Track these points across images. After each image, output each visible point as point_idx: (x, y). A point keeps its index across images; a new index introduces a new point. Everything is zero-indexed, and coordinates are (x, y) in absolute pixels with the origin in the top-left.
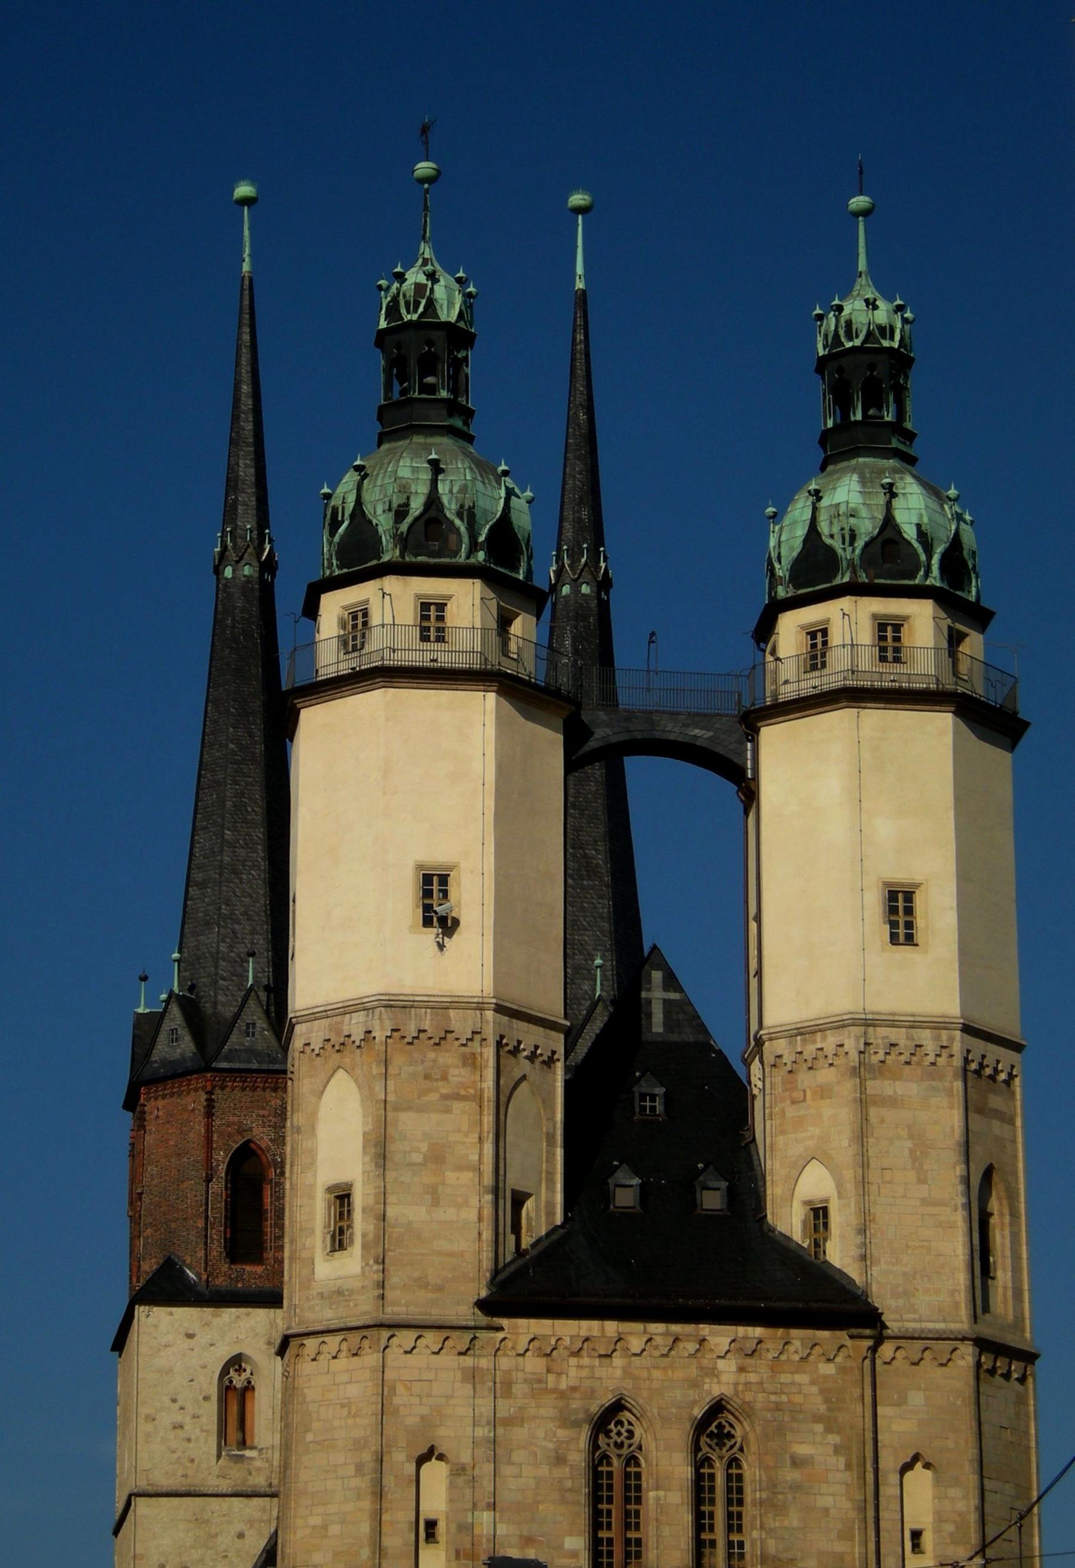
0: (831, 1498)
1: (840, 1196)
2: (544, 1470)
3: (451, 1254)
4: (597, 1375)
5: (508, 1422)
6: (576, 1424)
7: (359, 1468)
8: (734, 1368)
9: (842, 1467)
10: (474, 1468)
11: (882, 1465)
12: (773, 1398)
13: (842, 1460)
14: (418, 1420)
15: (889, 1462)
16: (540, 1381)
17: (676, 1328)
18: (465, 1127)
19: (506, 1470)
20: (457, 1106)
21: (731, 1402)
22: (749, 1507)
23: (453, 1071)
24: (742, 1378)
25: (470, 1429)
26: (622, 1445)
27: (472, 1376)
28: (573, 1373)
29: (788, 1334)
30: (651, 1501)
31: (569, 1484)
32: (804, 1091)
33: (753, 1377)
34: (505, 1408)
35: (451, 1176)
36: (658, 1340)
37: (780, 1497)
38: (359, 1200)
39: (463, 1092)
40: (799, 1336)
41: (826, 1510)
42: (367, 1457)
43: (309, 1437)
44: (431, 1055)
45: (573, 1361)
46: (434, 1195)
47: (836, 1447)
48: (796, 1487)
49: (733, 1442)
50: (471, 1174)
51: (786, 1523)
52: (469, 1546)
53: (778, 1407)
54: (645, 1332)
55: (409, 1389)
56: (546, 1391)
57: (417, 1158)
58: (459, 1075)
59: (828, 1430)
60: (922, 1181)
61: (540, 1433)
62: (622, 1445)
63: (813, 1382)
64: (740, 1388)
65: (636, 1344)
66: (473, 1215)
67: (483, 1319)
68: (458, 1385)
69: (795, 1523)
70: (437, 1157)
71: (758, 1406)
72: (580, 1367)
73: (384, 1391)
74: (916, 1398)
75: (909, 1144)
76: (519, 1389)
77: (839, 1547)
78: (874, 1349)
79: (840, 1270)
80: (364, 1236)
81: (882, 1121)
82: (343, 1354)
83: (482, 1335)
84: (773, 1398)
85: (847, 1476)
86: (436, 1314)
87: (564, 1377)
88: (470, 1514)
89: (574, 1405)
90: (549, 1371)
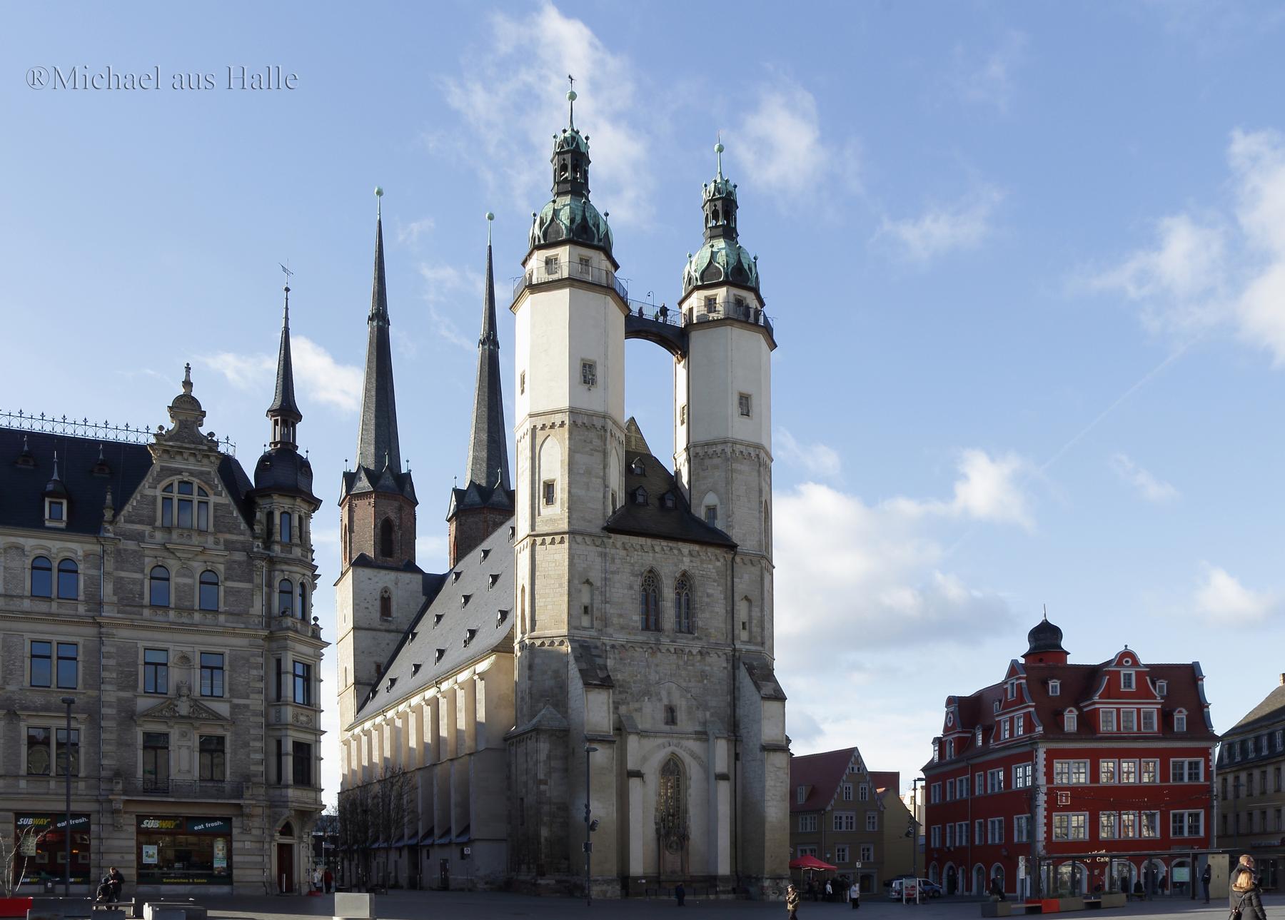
1: (721, 504)
3: (593, 509)
5: (613, 573)
6: (637, 576)
7: (561, 585)
8: (688, 561)
11: (735, 599)
12: (701, 572)
15: (736, 598)
17: (670, 544)
19: (613, 590)
27: (604, 556)
28: (636, 557)
31: (634, 597)
33: (695, 565)
34: (613, 568)
35: (594, 479)
36: (665, 548)
40: (711, 550)
41: (718, 613)
45: (636, 552)
48: (708, 604)
55: (579, 557)
56: (627, 562)
57: (582, 472)
59: (718, 585)
60: (749, 501)
63: (714, 568)
65: (657, 549)
69: (708, 616)
72: (637, 555)
74: (746, 577)
78: (733, 559)
79: (720, 531)
80: (561, 499)
81: (737, 479)
83: (605, 540)
85: (724, 602)
89: (636, 569)
90: (627, 556)
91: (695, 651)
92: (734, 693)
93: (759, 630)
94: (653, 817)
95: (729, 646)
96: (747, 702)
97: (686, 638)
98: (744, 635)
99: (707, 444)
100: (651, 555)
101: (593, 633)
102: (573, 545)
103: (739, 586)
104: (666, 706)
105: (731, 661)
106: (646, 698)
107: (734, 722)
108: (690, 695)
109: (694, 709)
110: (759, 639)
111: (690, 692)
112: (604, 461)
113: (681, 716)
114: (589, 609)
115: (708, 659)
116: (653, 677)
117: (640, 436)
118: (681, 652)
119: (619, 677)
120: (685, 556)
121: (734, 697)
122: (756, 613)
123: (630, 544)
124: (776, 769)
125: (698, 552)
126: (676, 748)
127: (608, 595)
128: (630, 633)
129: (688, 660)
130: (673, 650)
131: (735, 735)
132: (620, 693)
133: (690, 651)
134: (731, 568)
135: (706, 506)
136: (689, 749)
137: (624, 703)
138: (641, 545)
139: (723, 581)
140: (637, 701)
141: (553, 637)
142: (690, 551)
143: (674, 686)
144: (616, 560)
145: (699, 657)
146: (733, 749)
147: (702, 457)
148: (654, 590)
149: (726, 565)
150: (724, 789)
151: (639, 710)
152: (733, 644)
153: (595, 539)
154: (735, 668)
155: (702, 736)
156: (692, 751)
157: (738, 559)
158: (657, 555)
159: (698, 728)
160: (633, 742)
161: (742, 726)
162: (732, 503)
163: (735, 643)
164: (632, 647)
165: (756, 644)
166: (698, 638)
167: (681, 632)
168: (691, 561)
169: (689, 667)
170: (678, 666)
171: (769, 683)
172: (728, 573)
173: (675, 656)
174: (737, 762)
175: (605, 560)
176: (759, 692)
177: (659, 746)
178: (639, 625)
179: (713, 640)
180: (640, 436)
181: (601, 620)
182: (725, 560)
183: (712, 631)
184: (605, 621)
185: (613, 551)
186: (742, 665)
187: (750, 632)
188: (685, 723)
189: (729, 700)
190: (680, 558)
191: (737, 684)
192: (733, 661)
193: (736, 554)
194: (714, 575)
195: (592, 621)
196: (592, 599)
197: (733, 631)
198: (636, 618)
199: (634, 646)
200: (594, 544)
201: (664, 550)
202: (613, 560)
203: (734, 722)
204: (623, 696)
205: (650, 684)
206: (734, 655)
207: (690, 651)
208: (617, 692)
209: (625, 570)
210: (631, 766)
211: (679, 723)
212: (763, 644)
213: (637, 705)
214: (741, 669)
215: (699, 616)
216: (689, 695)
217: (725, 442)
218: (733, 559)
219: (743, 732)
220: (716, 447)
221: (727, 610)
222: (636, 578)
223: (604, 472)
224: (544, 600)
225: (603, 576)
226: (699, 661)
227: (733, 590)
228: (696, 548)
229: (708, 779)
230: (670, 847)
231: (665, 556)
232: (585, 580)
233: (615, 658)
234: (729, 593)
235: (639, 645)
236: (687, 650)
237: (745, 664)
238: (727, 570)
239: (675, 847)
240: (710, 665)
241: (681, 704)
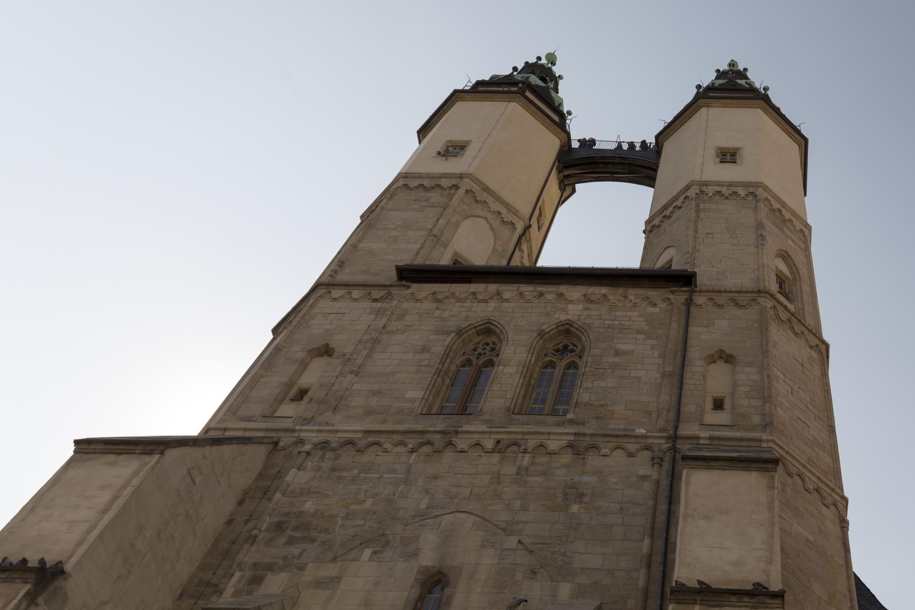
12: (606, 322)
21: (574, 325)
24: (586, 313)
41: (639, 378)
65: (507, 295)
83: (395, 291)
84: (606, 322)
103: (702, 337)
108: (515, 539)
109: (519, 576)
115: (593, 461)
120: (572, 302)
129: (532, 463)
130: (489, 444)
158: (506, 304)
170: (498, 478)
173: (496, 458)
231: (526, 305)
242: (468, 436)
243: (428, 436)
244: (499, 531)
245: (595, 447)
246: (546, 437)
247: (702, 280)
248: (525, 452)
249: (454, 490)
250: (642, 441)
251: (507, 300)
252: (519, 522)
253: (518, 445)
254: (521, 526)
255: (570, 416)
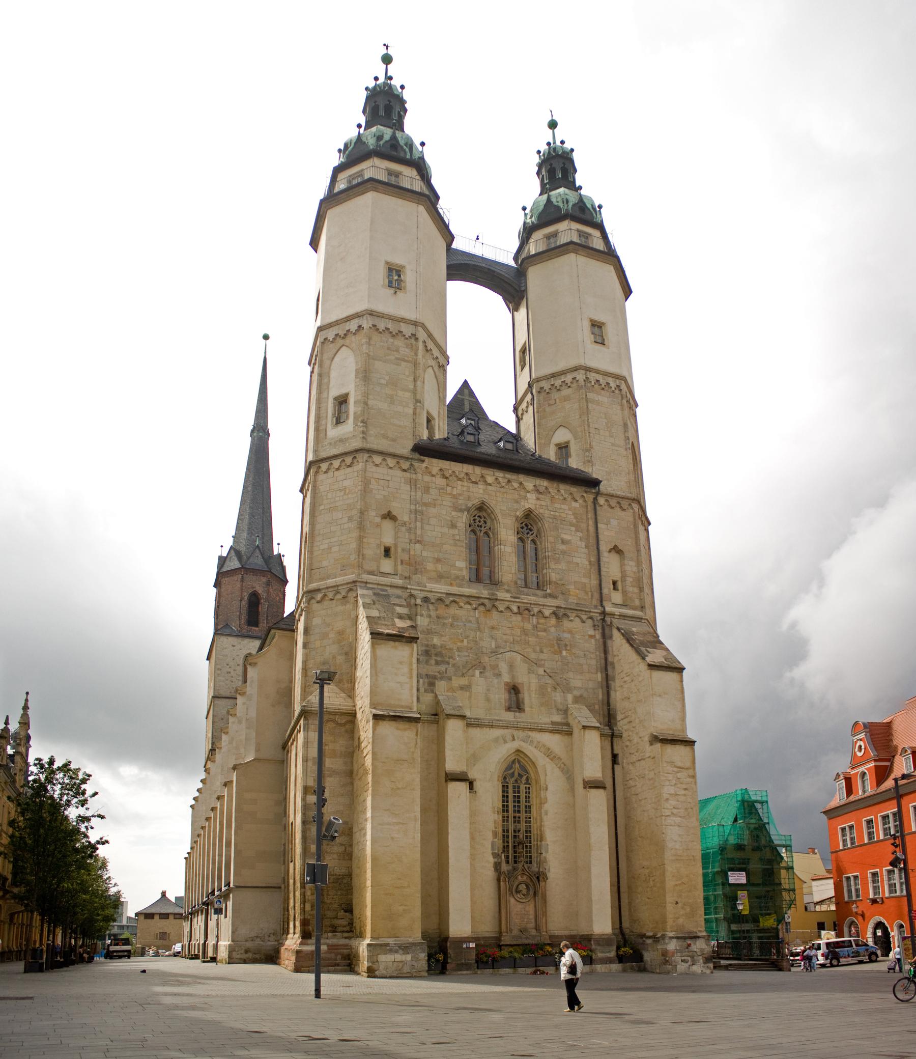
0: (579, 559)
1: (576, 438)
2: (445, 530)
3: (400, 426)
4: (471, 490)
6: (461, 511)
7: (350, 519)
8: (535, 498)
9: (584, 547)
10: (410, 524)
12: (552, 513)
13: (584, 544)
14: (382, 497)
15: (604, 548)
16: (443, 489)
18: (407, 373)
19: (427, 527)
20: (404, 364)
22: (541, 561)
23: (401, 349)
24: (538, 502)
25: (408, 506)
26: (481, 526)
28: (460, 487)
29: (559, 487)
30: (496, 551)
31: (458, 537)
32: (555, 400)
33: (543, 503)
34: (427, 498)
35: (400, 393)
36: (501, 480)
37: (557, 555)
38: (351, 400)
39: (406, 358)
41: (578, 564)
42: (355, 512)
43: (322, 507)
44: (391, 340)
45: (459, 483)
46: (391, 399)
47: (580, 537)
48: (564, 553)
49: (532, 532)
50: (410, 394)
51: (560, 567)
52: (408, 559)
53: (555, 518)
54: (494, 475)
58: (405, 351)
59: (577, 530)
61: (444, 512)
62: (481, 526)
64: (537, 506)
65: (490, 479)
66: (411, 411)
67: (417, 456)
68: (402, 484)
70: (394, 383)
71: (546, 515)
73: (366, 483)
74: (614, 522)
75: (605, 420)
76: (433, 491)
77: (584, 580)
78: (595, 499)
80: (355, 413)
82: (342, 468)
83: (416, 464)
85: (586, 551)
86: (392, 450)
87: (455, 489)
88: (408, 545)
89: (460, 502)
90: (447, 485)
91: (547, 612)
92: (606, 670)
93: (636, 590)
94: (490, 846)
95: (596, 607)
96: (626, 679)
97: (534, 595)
98: (617, 597)
99: (553, 375)
100: (481, 486)
101: (399, 582)
102: (368, 467)
104: (507, 684)
105: (600, 631)
106: (477, 672)
107: (609, 710)
110: (637, 603)
111: (543, 666)
112: (415, 373)
113: (530, 698)
114: (392, 550)
115: (566, 624)
116: (488, 644)
117: (475, 400)
118: (527, 612)
119: (436, 641)
120: (528, 492)
121: (607, 675)
122: (631, 567)
123: (450, 472)
124: (676, 769)
125: (546, 488)
126: (523, 744)
127: (419, 532)
128: (451, 585)
129: (538, 623)
130: (515, 609)
131: (611, 728)
132: (437, 663)
133: (540, 612)
134: (593, 512)
135: (556, 445)
136: (544, 746)
137: (441, 678)
138: (467, 474)
139: (583, 526)
140: (463, 675)
141: (338, 586)
142: (535, 486)
143: (519, 657)
144: (431, 490)
145: (553, 621)
146: (609, 748)
147: (547, 391)
148: (486, 533)
149: (587, 506)
150: (598, 801)
151: (466, 688)
152: (602, 605)
153: (401, 461)
154: (606, 637)
155: (564, 730)
156: (549, 749)
157: (601, 500)
159: (557, 718)
160: (453, 728)
161: (619, 717)
162: (590, 436)
163: (605, 603)
164: (454, 601)
165: (635, 609)
166: (551, 596)
167: (526, 586)
168: (538, 499)
169: (539, 633)
170: (525, 632)
171: (655, 650)
172: (590, 516)
173: (519, 618)
174: (616, 766)
175: (416, 489)
176: (644, 658)
177: (496, 740)
178: (465, 573)
179: (572, 600)
180: (475, 400)
181: (409, 564)
182: (585, 501)
183: (572, 587)
184: (415, 566)
185: (427, 478)
186: (615, 633)
187: (625, 593)
188: (534, 712)
189: (600, 679)
190: (522, 493)
191: (610, 659)
192: (603, 629)
193: (598, 493)
194: (571, 518)
195: (395, 565)
196: (396, 537)
197: (601, 589)
198: (461, 565)
199: (458, 600)
200: (400, 468)
201: (499, 483)
202: (427, 490)
203: (609, 710)
204: (442, 668)
205: (482, 653)
206: (603, 620)
207: (540, 612)
208: (433, 662)
209: (445, 503)
210: (452, 764)
211: (527, 709)
212: (642, 608)
213: (464, 681)
214: (614, 638)
215: (552, 566)
216: (541, 671)
217: (576, 369)
218: (595, 499)
219: (622, 725)
220: (566, 377)
221: (590, 562)
222: (459, 514)
223: (415, 386)
224: (328, 541)
225: (413, 507)
226: (555, 626)
227: (597, 537)
228: (544, 483)
229: (572, 789)
230: (518, 892)
231: (502, 490)
232: (386, 512)
233: (430, 616)
234: (592, 541)
235: (466, 599)
236: (536, 610)
237: (619, 629)
238: (587, 512)
239: (524, 891)
240: (570, 632)
241: (529, 683)
242: (502, 602)
243: (482, 600)
244: (534, 664)
245: (565, 615)
246: (542, 607)
247: (602, 487)
248: (533, 615)
249: (505, 637)
250: (588, 614)
251: (490, 484)
252: (542, 660)
253: (529, 611)
254: (543, 662)
255: (548, 591)
